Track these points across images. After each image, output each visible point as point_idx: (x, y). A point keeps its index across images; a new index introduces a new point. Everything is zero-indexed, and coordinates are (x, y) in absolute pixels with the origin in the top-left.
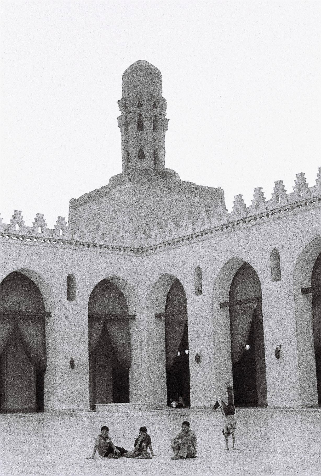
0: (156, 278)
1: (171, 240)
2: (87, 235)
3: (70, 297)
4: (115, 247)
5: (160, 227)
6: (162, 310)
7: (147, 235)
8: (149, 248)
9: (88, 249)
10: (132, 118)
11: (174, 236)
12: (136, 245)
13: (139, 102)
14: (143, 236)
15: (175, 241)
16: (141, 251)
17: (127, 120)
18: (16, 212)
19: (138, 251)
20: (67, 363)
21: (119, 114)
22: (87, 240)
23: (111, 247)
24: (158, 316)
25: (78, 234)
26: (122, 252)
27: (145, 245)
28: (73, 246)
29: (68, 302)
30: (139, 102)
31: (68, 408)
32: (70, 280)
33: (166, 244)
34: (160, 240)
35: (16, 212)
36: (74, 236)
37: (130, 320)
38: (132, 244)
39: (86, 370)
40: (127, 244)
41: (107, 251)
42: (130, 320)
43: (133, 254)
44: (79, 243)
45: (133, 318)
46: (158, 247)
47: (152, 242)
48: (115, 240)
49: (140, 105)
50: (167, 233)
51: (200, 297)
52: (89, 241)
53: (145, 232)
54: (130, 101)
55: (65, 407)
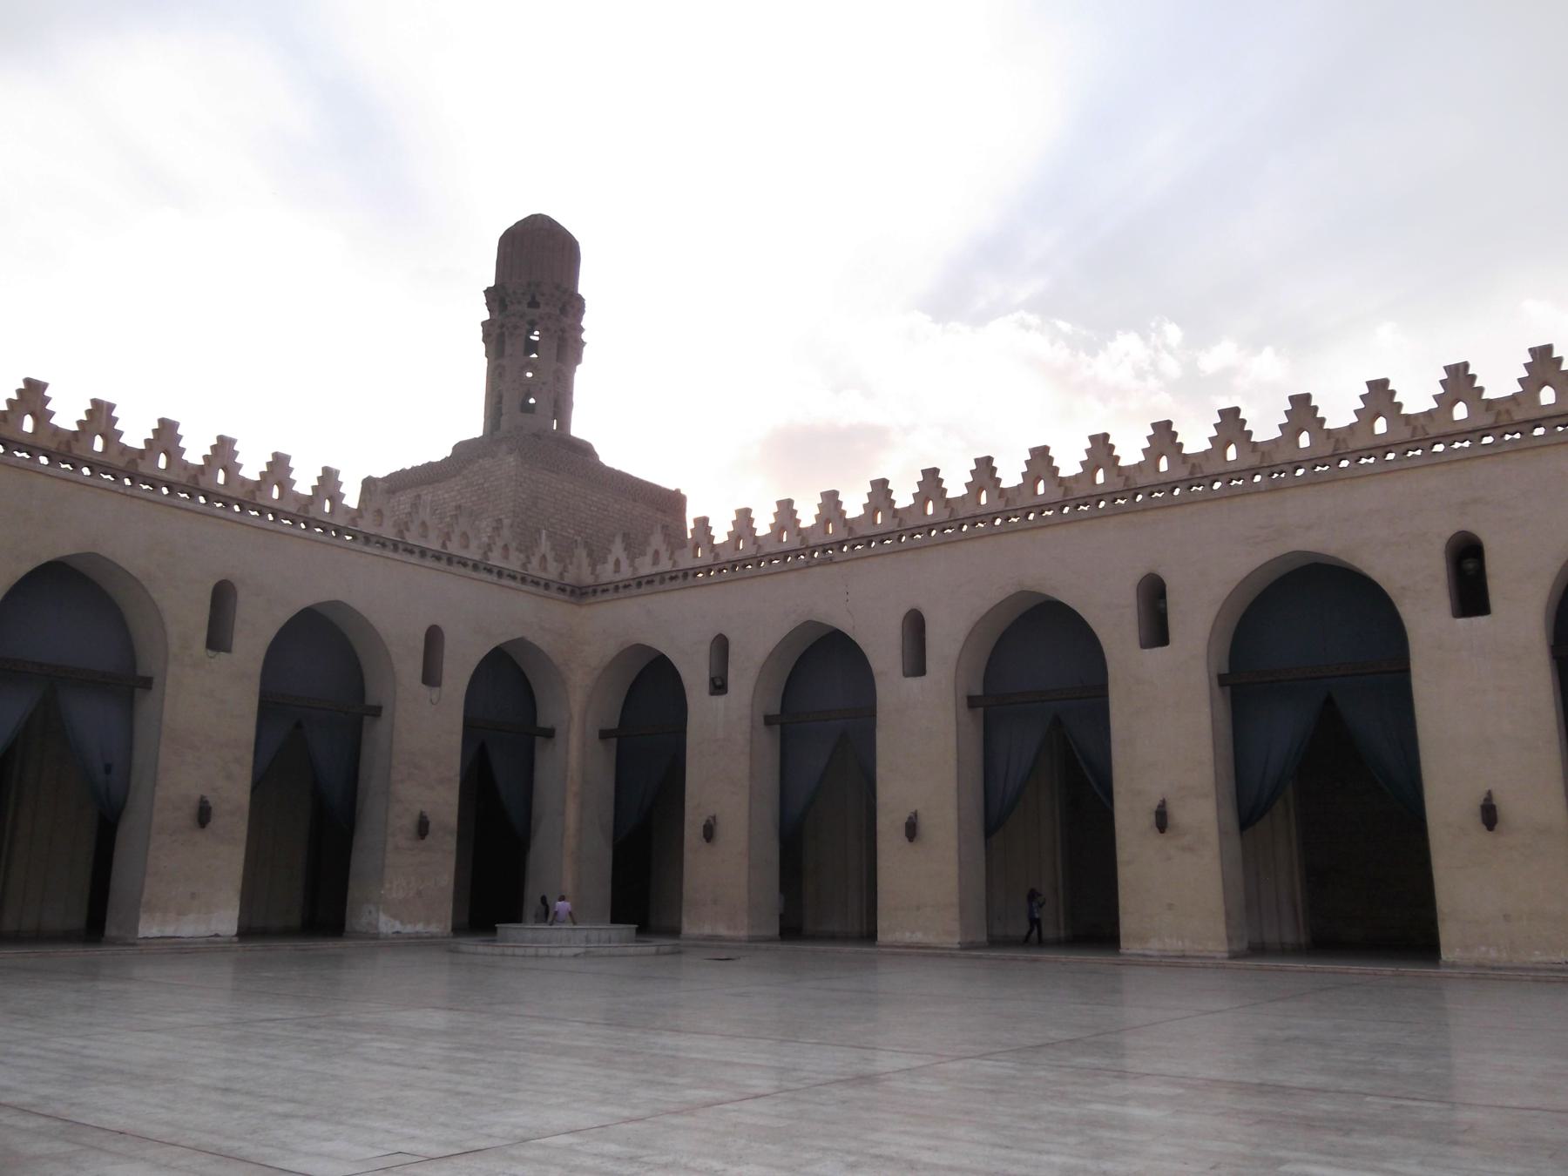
0: (612, 650)
1: (656, 574)
2: (474, 544)
3: (431, 676)
4: (529, 579)
5: (628, 547)
6: (614, 723)
7: (596, 558)
8: (600, 589)
9: (474, 575)
10: (516, 327)
11: (665, 565)
12: (569, 578)
13: (533, 297)
14: (585, 561)
15: (667, 576)
16: (579, 593)
17: (504, 329)
18: (326, 470)
19: (573, 592)
20: (409, 822)
21: (486, 316)
22: (473, 554)
23: (519, 576)
24: (604, 735)
25: (455, 538)
26: (541, 591)
27: (588, 579)
28: (443, 565)
29: (424, 686)
30: (533, 297)
31: (409, 929)
32: (434, 637)
33: (643, 583)
34: (626, 572)
35: (326, 470)
36: (448, 543)
37: (538, 740)
38: (561, 574)
39: (451, 843)
40: (552, 571)
41: (512, 584)
42: (538, 740)
43: (561, 596)
44: (455, 560)
45: (549, 734)
46: (621, 585)
47: (607, 573)
48: (530, 562)
49: (533, 304)
50: (648, 559)
51: (720, 701)
52: (477, 557)
53: (590, 555)
54: (514, 292)
55: (398, 927)
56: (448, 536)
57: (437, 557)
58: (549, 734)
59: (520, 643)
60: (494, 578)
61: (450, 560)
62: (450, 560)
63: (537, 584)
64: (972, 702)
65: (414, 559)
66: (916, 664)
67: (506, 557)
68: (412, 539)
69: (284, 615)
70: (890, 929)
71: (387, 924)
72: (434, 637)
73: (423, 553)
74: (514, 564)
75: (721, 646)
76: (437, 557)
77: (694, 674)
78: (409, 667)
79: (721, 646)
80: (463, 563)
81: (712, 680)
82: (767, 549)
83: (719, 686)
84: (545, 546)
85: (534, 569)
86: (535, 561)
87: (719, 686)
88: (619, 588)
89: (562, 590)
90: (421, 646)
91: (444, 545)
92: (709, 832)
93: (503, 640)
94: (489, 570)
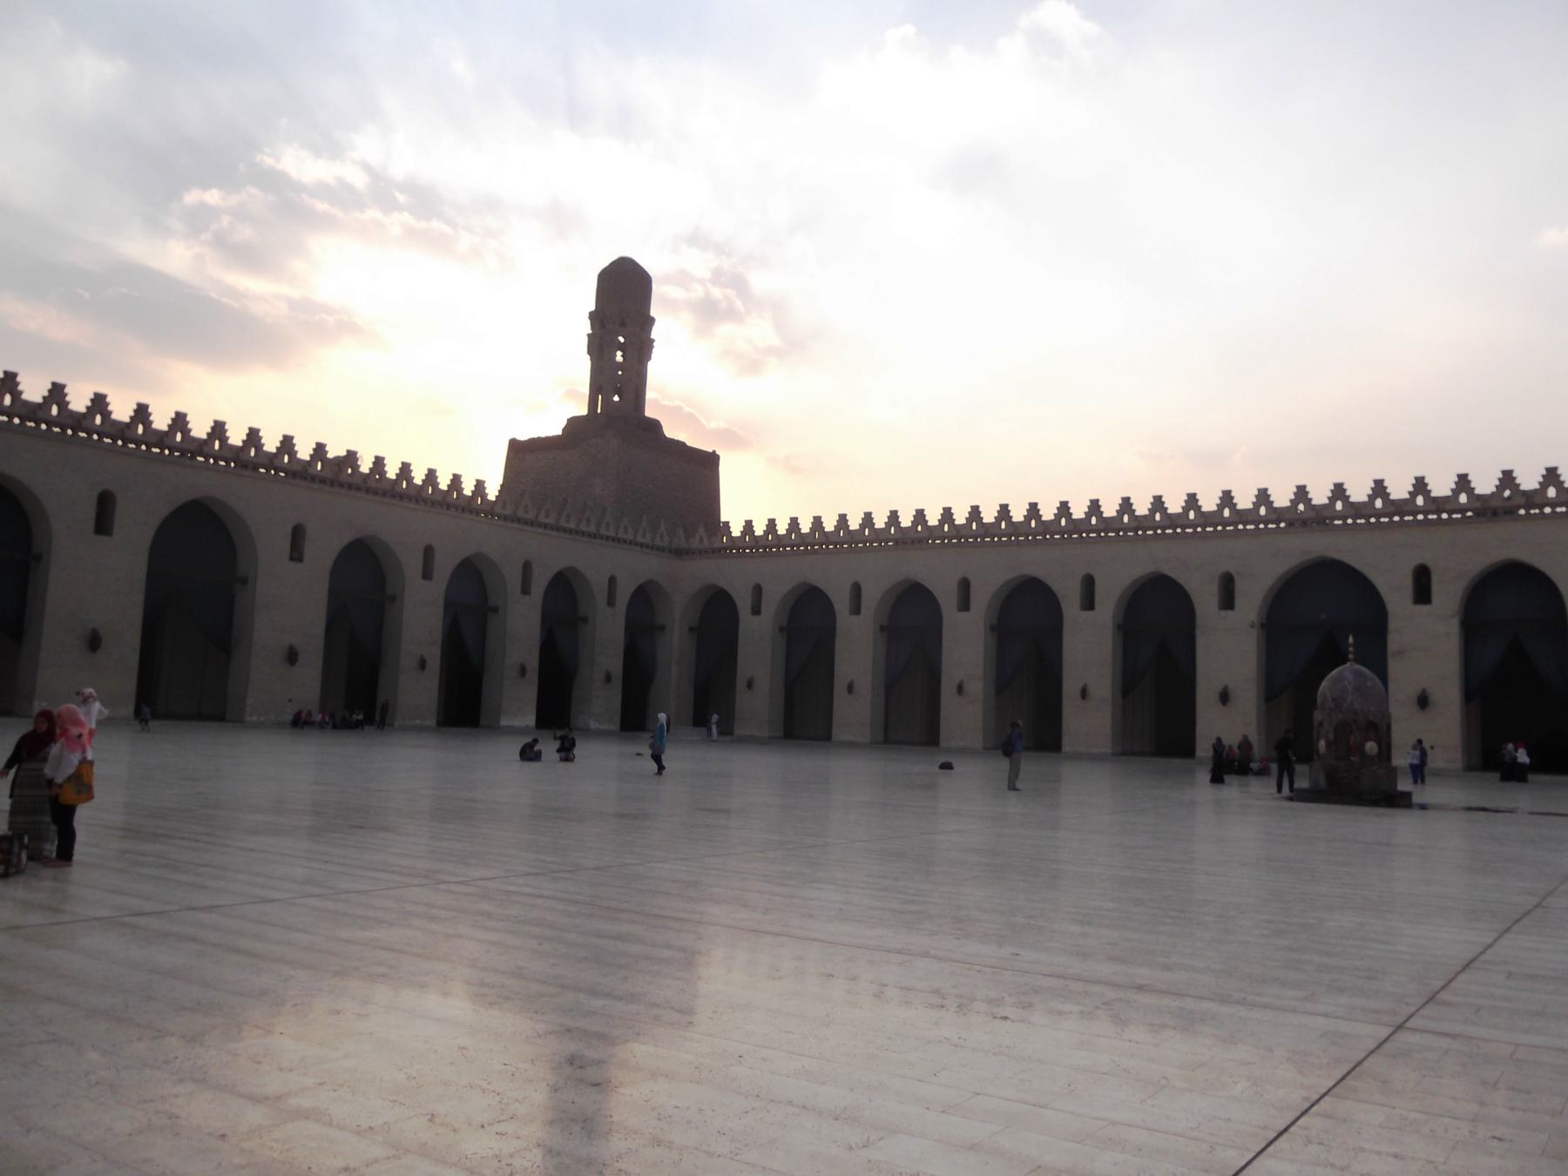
16: (680, 553)
31: (602, 727)
32: (612, 581)
34: (706, 543)
39: (619, 685)
40: (666, 544)
45: (662, 628)
51: (756, 619)
55: (597, 726)
56: (618, 529)
57: (613, 540)
58: (662, 628)
59: (651, 582)
60: (639, 549)
61: (619, 540)
62: (619, 540)
63: (658, 549)
64: (882, 628)
65: (604, 542)
66: (856, 609)
67: (644, 536)
68: (603, 532)
69: (550, 575)
70: (839, 733)
71: (593, 725)
72: (612, 581)
73: (607, 538)
74: (648, 540)
75: (758, 591)
76: (613, 540)
77: (743, 603)
78: (601, 599)
79: (758, 591)
80: (625, 542)
81: (753, 608)
82: (784, 542)
83: (756, 610)
84: (663, 528)
85: (658, 542)
86: (658, 537)
87: (756, 610)
88: (703, 553)
89: (670, 551)
90: (606, 586)
91: (617, 534)
92: (750, 685)
93: (642, 581)
94: (636, 544)
